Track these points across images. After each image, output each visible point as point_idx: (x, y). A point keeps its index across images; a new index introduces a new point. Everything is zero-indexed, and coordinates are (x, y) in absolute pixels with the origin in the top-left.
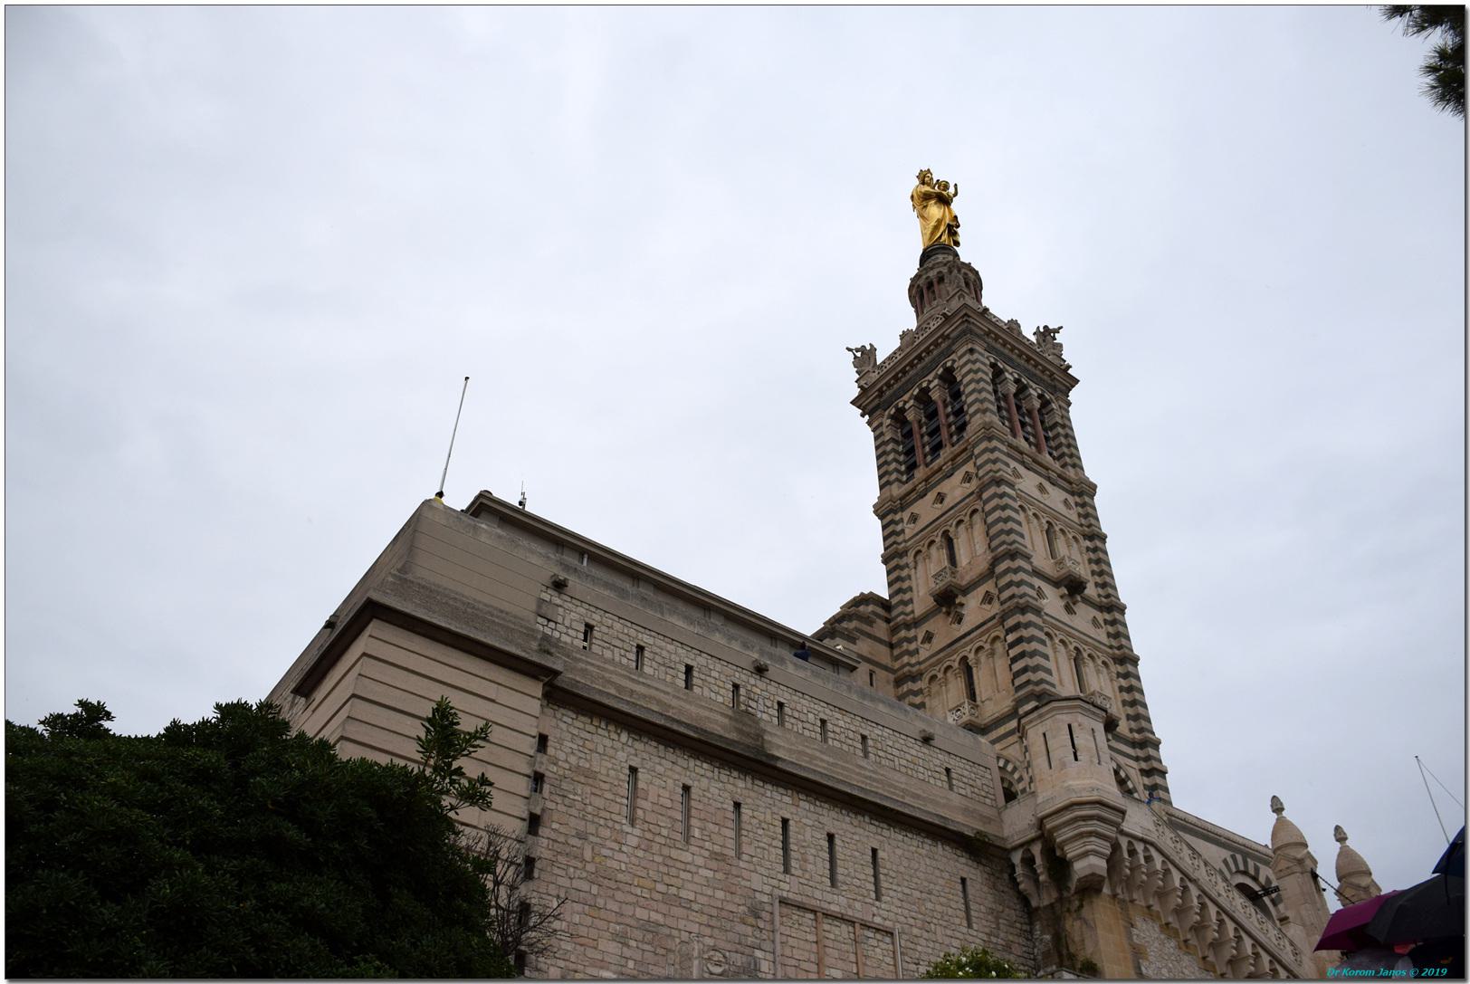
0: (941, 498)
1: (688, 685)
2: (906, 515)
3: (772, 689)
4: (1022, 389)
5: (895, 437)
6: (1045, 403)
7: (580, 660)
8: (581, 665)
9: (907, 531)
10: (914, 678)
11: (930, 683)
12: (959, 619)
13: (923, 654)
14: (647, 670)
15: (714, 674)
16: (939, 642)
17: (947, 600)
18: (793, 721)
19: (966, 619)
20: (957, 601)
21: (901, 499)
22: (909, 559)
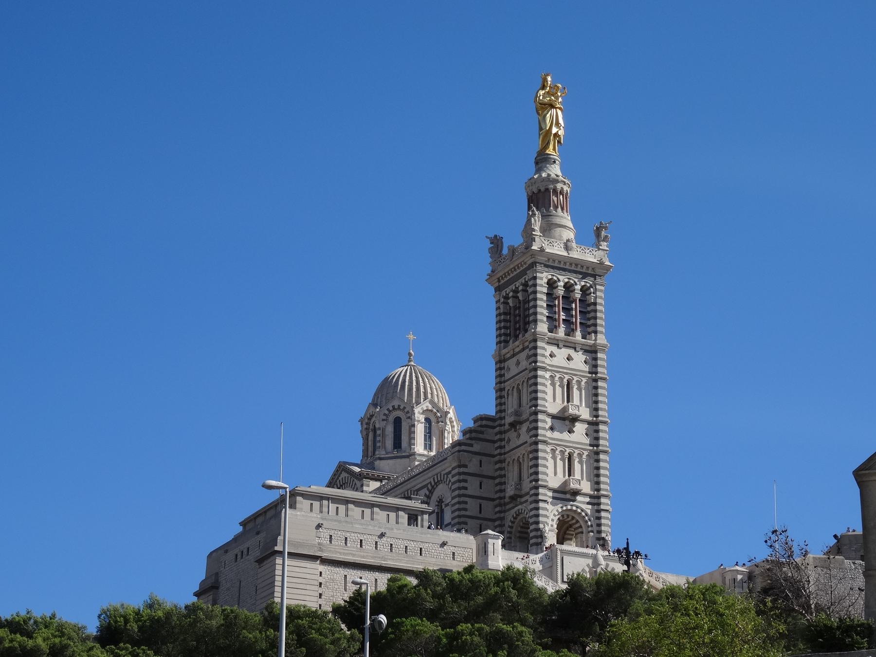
0: (518, 363)
1: (361, 546)
2: (506, 364)
3: (389, 540)
4: (568, 287)
5: (506, 311)
6: (584, 290)
7: (329, 548)
8: (329, 549)
9: (506, 375)
10: (501, 462)
11: (508, 465)
12: (520, 435)
13: (507, 449)
14: (348, 545)
15: (370, 540)
16: (512, 445)
17: (514, 425)
18: (395, 549)
19: (522, 437)
20: (518, 428)
21: (504, 355)
22: (505, 393)
